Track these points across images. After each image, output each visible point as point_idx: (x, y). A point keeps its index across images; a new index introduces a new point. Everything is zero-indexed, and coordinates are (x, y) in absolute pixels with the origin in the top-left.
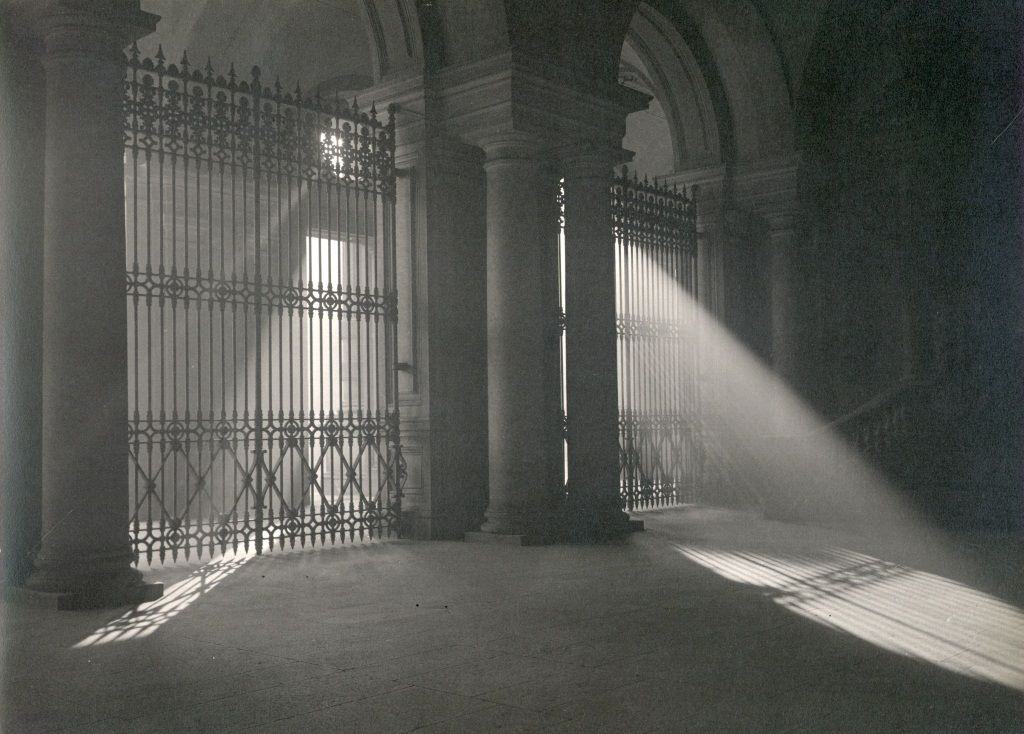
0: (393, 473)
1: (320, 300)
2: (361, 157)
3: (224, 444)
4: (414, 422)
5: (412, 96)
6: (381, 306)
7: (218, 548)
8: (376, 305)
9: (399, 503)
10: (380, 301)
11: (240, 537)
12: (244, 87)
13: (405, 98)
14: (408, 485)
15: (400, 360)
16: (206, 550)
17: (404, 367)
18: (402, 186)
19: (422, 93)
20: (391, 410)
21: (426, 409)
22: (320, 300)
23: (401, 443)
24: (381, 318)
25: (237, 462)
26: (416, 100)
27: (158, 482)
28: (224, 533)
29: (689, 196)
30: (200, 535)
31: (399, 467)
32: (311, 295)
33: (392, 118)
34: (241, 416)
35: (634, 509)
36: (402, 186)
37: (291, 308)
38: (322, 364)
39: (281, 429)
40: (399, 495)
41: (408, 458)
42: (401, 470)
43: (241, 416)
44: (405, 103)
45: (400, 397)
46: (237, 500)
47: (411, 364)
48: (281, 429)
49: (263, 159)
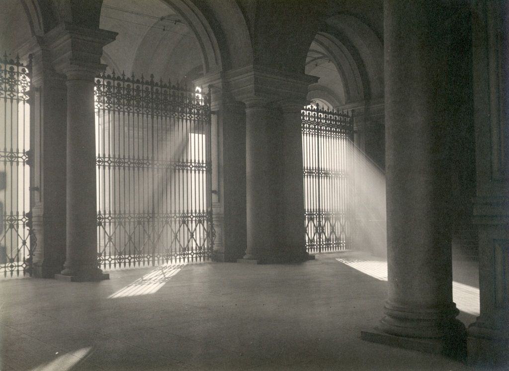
0: (210, 234)
1: (195, 167)
2: (107, 94)
3: (167, 222)
4: (218, 214)
5: (217, 81)
6: (205, 167)
7: (165, 261)
8: (203, 167)
9: (212, 247)
10: (204, 165)
11: (173, 257)
12: (147, 83)
13: (214, 82)
14: (216, 240)
15: (212, 190)
16: (161, 262)
17: (214, 192)
18: (214, 118)
19: (221, 80)
20: (209, 210)
21: (222, 209)
22: (195, 167)
23: (213, 223)
24: (205, 172)
25: (172, 229)
26: (219, 83)
27: (133, 236)
28: (120, 259)
29: (350, 114)
30: (110, 260)
31: (212, 233)
32: (191, 164)
33: (210, 90)
34: (173, 212)
35: (322, 251)
36: (214, 118)
37: (183, 170)
38: (195, 192)
39: (196, 217)
40: (212, 244)
41: (216, 229)
42: (213, 235)
43: (173, 212)
44: (215, 84)
45: (213, 204)
46: (172, 243)
47: (217, 191)
48: (196, 217)
49: (155, 111)
